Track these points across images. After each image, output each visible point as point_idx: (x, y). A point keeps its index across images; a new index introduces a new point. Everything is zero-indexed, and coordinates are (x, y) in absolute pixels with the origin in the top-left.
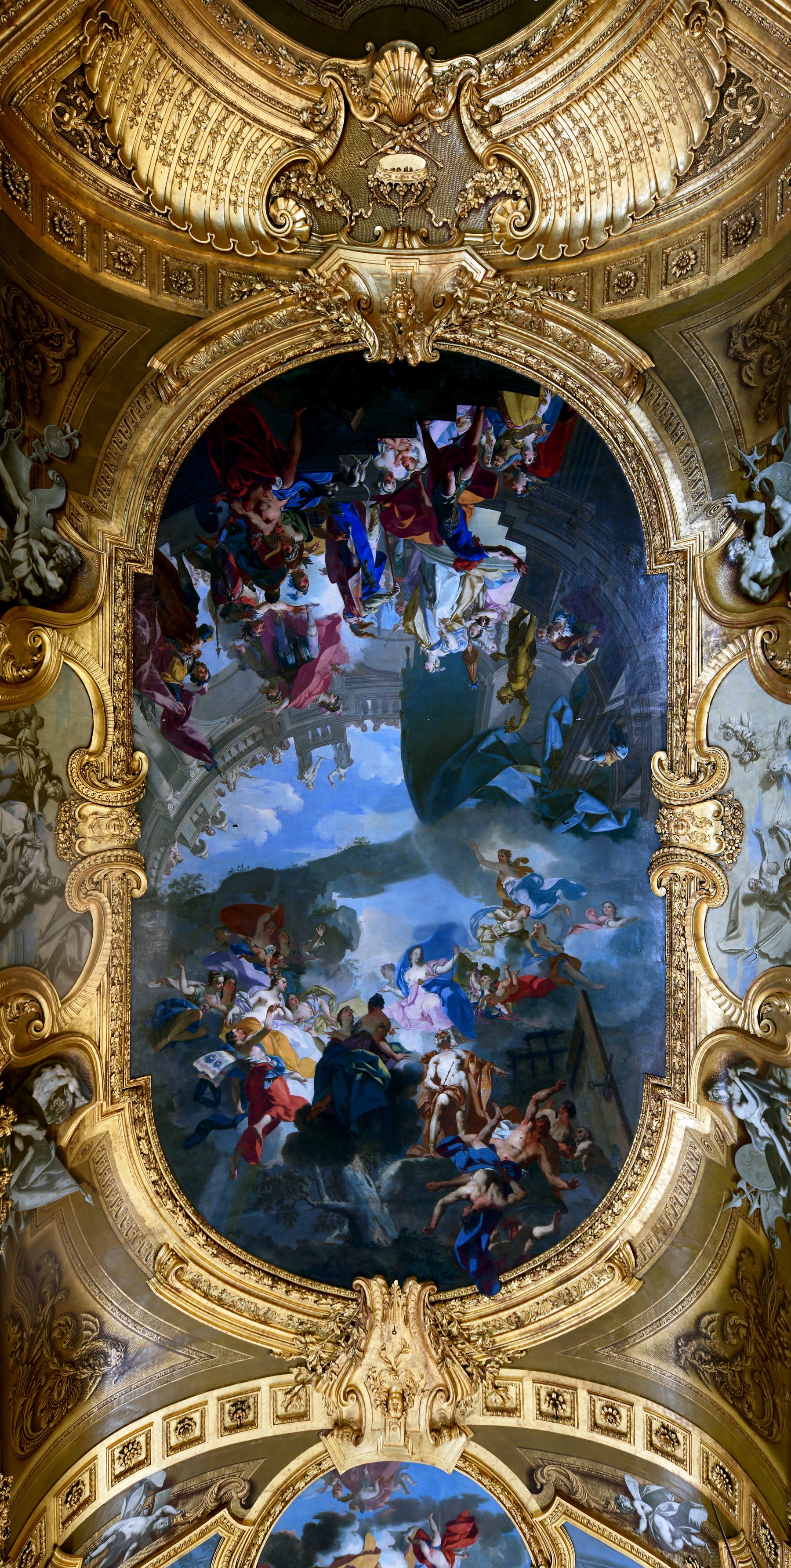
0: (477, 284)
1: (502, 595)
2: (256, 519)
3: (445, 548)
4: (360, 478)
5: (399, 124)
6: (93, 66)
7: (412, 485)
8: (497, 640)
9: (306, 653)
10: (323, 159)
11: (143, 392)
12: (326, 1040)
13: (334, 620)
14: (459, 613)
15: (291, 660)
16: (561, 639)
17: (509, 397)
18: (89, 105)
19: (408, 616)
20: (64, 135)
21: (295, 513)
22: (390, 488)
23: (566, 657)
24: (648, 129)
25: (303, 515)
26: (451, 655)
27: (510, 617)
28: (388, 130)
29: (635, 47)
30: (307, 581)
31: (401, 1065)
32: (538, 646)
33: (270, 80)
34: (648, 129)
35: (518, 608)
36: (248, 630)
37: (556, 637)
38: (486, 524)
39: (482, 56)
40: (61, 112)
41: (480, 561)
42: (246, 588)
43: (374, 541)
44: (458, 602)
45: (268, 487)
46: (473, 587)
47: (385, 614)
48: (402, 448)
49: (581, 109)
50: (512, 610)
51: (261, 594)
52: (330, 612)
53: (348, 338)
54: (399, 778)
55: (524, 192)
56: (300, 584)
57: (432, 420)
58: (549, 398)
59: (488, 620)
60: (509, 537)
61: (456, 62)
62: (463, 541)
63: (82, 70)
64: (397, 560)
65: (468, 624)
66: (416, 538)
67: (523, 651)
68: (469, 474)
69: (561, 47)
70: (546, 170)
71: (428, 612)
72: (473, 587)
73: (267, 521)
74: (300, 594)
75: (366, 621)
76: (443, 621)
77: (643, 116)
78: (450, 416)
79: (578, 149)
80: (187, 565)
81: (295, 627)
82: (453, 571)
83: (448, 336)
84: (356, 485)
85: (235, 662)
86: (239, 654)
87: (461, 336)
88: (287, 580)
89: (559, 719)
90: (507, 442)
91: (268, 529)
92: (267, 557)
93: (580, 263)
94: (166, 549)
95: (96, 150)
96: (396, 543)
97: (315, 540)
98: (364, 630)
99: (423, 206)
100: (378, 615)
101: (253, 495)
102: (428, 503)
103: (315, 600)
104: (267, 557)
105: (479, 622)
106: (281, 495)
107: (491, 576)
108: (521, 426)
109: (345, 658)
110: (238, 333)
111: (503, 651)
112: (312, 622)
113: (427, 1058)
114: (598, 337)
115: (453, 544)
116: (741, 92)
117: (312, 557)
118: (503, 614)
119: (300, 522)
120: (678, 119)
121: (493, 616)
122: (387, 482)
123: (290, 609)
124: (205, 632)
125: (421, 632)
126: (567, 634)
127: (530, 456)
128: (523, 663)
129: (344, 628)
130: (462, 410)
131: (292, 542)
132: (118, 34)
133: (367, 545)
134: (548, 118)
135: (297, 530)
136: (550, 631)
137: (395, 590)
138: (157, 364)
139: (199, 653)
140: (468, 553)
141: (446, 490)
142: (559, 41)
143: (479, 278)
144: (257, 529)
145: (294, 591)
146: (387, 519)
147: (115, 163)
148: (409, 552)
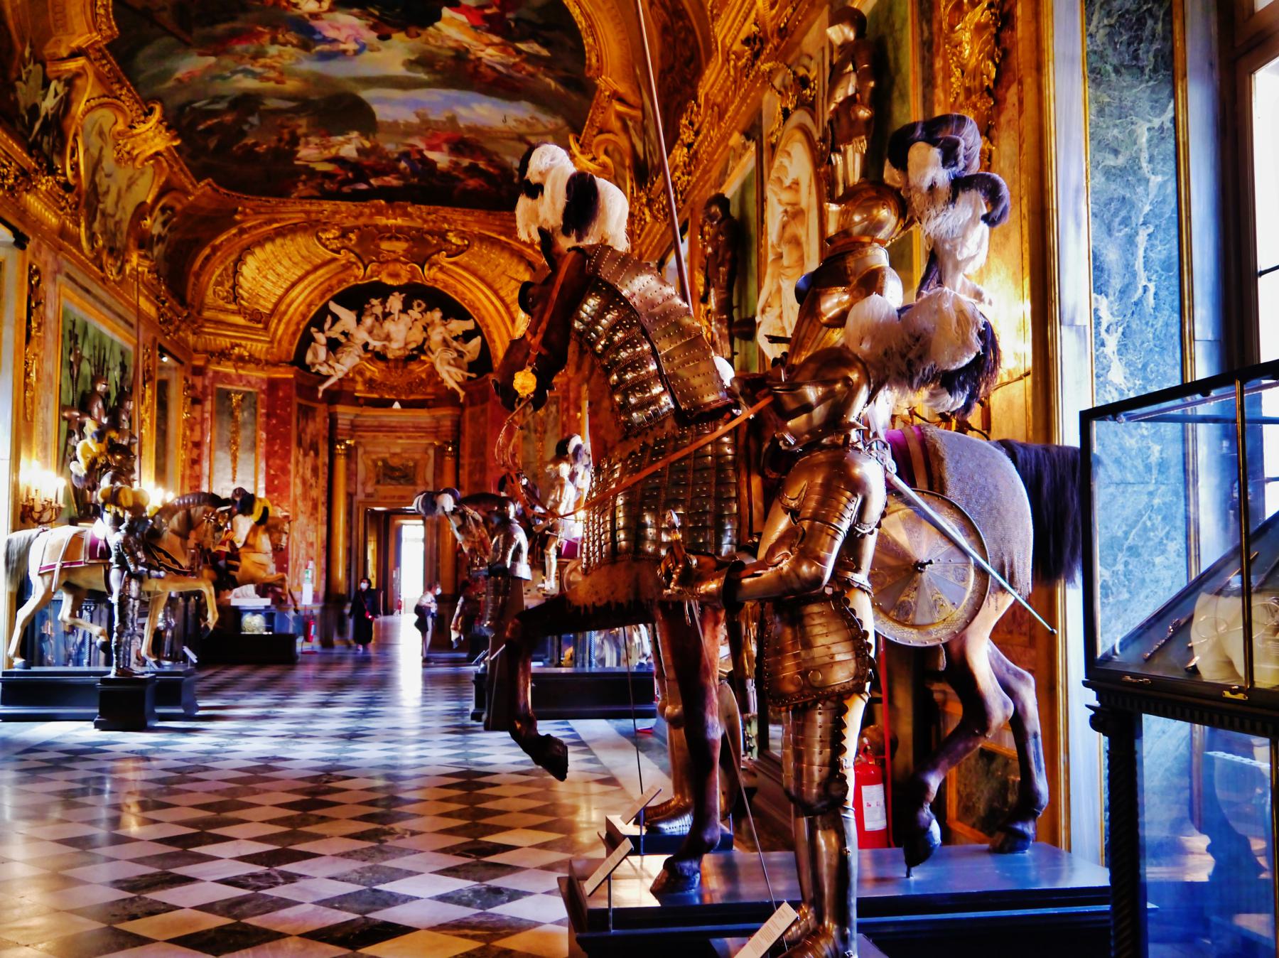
5: (397, 260)
12: (431, 29)
29: (281, 299)
31: (355, 10)
54: (376, 108)
89: (252, 126)
113: (330, 10)
128: (286, 136)
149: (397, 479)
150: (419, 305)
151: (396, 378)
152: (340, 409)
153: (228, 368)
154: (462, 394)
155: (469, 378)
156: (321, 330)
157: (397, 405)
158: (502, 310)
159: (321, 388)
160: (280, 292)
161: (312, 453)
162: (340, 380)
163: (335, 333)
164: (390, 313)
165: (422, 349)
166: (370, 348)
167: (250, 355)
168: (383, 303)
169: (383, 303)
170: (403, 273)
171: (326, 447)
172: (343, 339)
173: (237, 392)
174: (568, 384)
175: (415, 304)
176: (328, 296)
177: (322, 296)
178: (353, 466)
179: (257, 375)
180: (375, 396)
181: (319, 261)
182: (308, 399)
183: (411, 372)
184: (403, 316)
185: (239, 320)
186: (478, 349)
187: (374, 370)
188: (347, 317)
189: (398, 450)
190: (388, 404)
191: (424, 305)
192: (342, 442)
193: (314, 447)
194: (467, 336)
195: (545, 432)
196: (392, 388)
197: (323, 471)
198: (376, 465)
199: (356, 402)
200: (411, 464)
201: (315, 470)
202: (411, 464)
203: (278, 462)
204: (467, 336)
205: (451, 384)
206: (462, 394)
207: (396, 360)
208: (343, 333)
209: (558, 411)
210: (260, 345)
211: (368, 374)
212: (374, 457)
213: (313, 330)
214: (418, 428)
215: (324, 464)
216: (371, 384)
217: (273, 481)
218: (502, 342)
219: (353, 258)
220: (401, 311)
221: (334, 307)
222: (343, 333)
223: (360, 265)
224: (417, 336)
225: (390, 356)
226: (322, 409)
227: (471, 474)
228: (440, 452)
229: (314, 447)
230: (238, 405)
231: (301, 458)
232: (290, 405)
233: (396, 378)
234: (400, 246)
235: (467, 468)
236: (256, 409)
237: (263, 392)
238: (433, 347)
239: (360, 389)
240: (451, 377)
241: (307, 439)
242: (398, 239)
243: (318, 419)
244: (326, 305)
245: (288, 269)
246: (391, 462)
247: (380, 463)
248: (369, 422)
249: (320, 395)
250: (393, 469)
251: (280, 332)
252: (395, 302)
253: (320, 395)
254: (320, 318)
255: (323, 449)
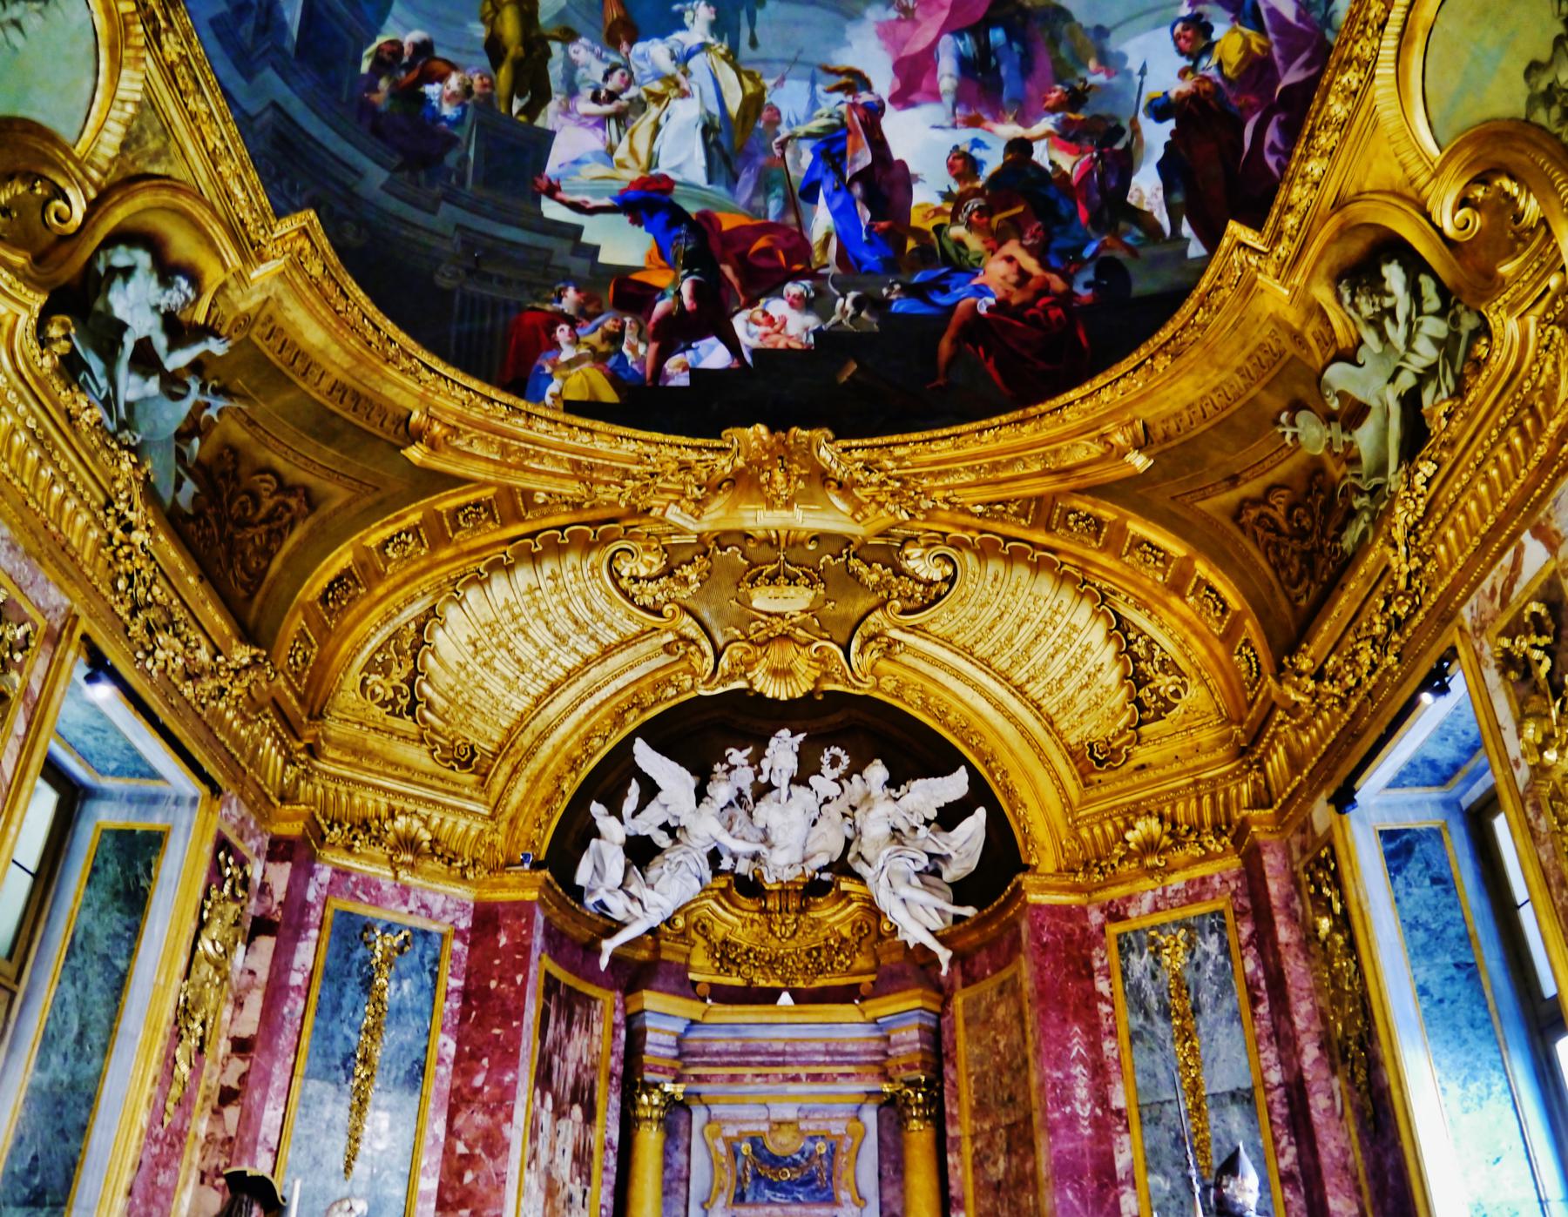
0: (677, 502)
1: (575, 147)
2: (1030, 264)
3: (692, 209)
4: (846, 303)
5: (786, 637)
6: (1127, 726)
7: (755, 292)
8: (571, 67)
9: (967, 45)
10: (878, 613)
11: (1167, 438)
13: (903, 99)
14: (653, 110)
15: (997, 36)
16: (442, 78)
17: (608, 395)
18: (1144, 693)
19: (754, 104)
20: (1181, 674)
21: (961, 266)
22: (792, 289)
23: (423, 49)
24: (487, 654)
25: (946, 259)
26: (663, 34)
27: (553, 106)
28: (799, 632)
29: (522, 722)
30: (951, 167)
32: (485, 61)
33: (935, 681)
34: (487, 654)
35: (539, 122)
36: (1076, 99)
37: (454, 81)
38: (623, 245)
39: (693, 694)
40: (1176, 694)
41: (623, 192)
42: (1067, 167)
43: (821, 220)
44: (657, 128)
45: (1002, 304)
46: (633, 152)
47: (799, 107)
48: (774, 337)
49: (571, 661)
50: (549, 118)
51: (1042, 154)
52: (910, 113)
53: (857, 454)
55: (624, 583)
56: (963, 164)
57: (727, 370)
58: (548, 400)
59: (595, 98)
60: (579, 229)
61: (720, 690)
62: (660, 219)
63: (1141, 723)
64: (779, 191)
65: (633, 92)
66: (744, 221)
67: (514, 50)
68: (660, 307)
69: (604, 710)
70: (600, 604)
71: (715, 110)
72: (633, 152)
73: (1010, 259)
74: (965, 148)
75: (839, 96)
76: (685, 94)
77: (497, 663)
78: (696, 374)
79: (565, 627)
80: (1164, 221)
81: (981, 90)
82: (673, 176)
83: (710, 456)
84: (852, 295)
85: (1113, 44)
86: (1104, 58)
87: (692, 456)
88: (987, 172)
90: (603, 348)
91: (1012, 248)
92: (1020, 209)
93: (537, 526)
94: (1196, 249)
95: (1150, 651)
96: (783, 213)
97: (929, 226)
98: (843, 80)
99: (752, 565)
100: (814, 104)
101: (1028, 295)
102: (728, 270)
103: (939, 135)
104: (1020, 209)
105: (612, 96)
106: (982, 291)
107: (601, 170)
108: (586, 367)
109: (886, 32)
110: (1019, 470)
111: (556, 47)
112: (948, 100)
114: (491, 467)
115: (679, 215)
116: (393, 702)
117: (938, 202)
118: (567, 112)
119: (952, 253)
120: (455, 668)
121: (585, 106)
122: (800, 297)
123: (989, 124)
124: (1161, 109)
125: (728, 76)
126: (432, 90)
127: (562, 333)
129: (883, 83)
130: (683, 380)
131: (970, 226)
132: (1091, 746)
133: (835, 214)
134: (607, 652)
135: (960, 243)
136: (468, 90)
137: (783, 145)
138: (1139, 462)
139: (1183, 74)
140: (648, 201)
141: (696, 287)
142: (607, 716)
143: (673, 508)
144: (1031, 251)
145: (977, 153)
146: (800, 248)
147: (1131, 636)
148: (759, 202)
149: (785, 1189)
150: (835, 762)
151: (790, 939)
152: (651, 1000)
153: (370, 864)
154: (944, 955)
155: (958, 919)
156: (615, 811)
157: (785, 999)
158: (1037, 728)
159: (609, 946)
160: (521, 704)
161: (577, 1111)
162: (652, 931)
163: (647, 824)
164: (770, 787)
165: (841, 867)
166: (726, 864)
167: (435, 841)
168: (755, 760)
169: (755, 760)
170: (801, 665)
171: (615, 1100)
172: (662, 839)
173: (389, 928)
174: (1253, 875)
175: (825, 759)
176: (633, 721)
177: (619, 718)
178: (680, 1157)
179: (445, 900)
180: (737, 981)
181: (614, 638)
182: (571, 968)
183: (817, 924)
184: (799, 791)
185: (418, 756)
186: (981, 837)
187: (734, 923)
188: (672, 777)
189: (790, 1113)
190: (771, 996)
191: (846, 760)
192: (649, 1087)
193: (583, 1096)
194: (949, 817)
195: (1196, 1010)
196: (773, 963)
197: (604, 1163)
198: (735, 1153)
199: (689, 990)
200: (822, 1147)
201: (582, 1158)
202: (822, 1147)
203: (480, 1119)
204: (949, 817)
205: (914, 933)
206: (944, 955)
207: (784, 892)
208: (665, 827)
209: (1226, 951)
210: (463, 823)
211: (720, 931)
212: (731, 1131)
213: (597, 809)
214: (835, 1054)
215: (608, 1145)
216: (725, 953)
217: (461, 1176)
218: (1042, 807)
219: (692, 630)
220: (793, 781)
221: (646, 757)
222: (665, 827)
223: (706, 645)
224: (828, 845)
225: (770, 882)
226: (607, 1001)
227: (980, 1162)
228: (892, 1110)
229: (583, 1096)
230: (388, 960)
231: (546, 1118)
232: (523, 966)
233: (790, 939)
234: (794, 600)
235: (967, 1148)
236: (435, 976)
237: (459, 934)
238: (868, 853)
239: (703, 970)
240: (918, 917)
241: (566, 1072)
242: (792, 580)
243: (597, 1028)
244: (626, 746)
245: (543, 654)
246: (770, 1146)
247: (746, 1148)
248: (721, 1041)
249: (604, 962)
250: (776, 1161)
251: (516, 798)
252: (783, 751)
253: (604, 962)
254: (612, 779)
255: (609, 1104)
